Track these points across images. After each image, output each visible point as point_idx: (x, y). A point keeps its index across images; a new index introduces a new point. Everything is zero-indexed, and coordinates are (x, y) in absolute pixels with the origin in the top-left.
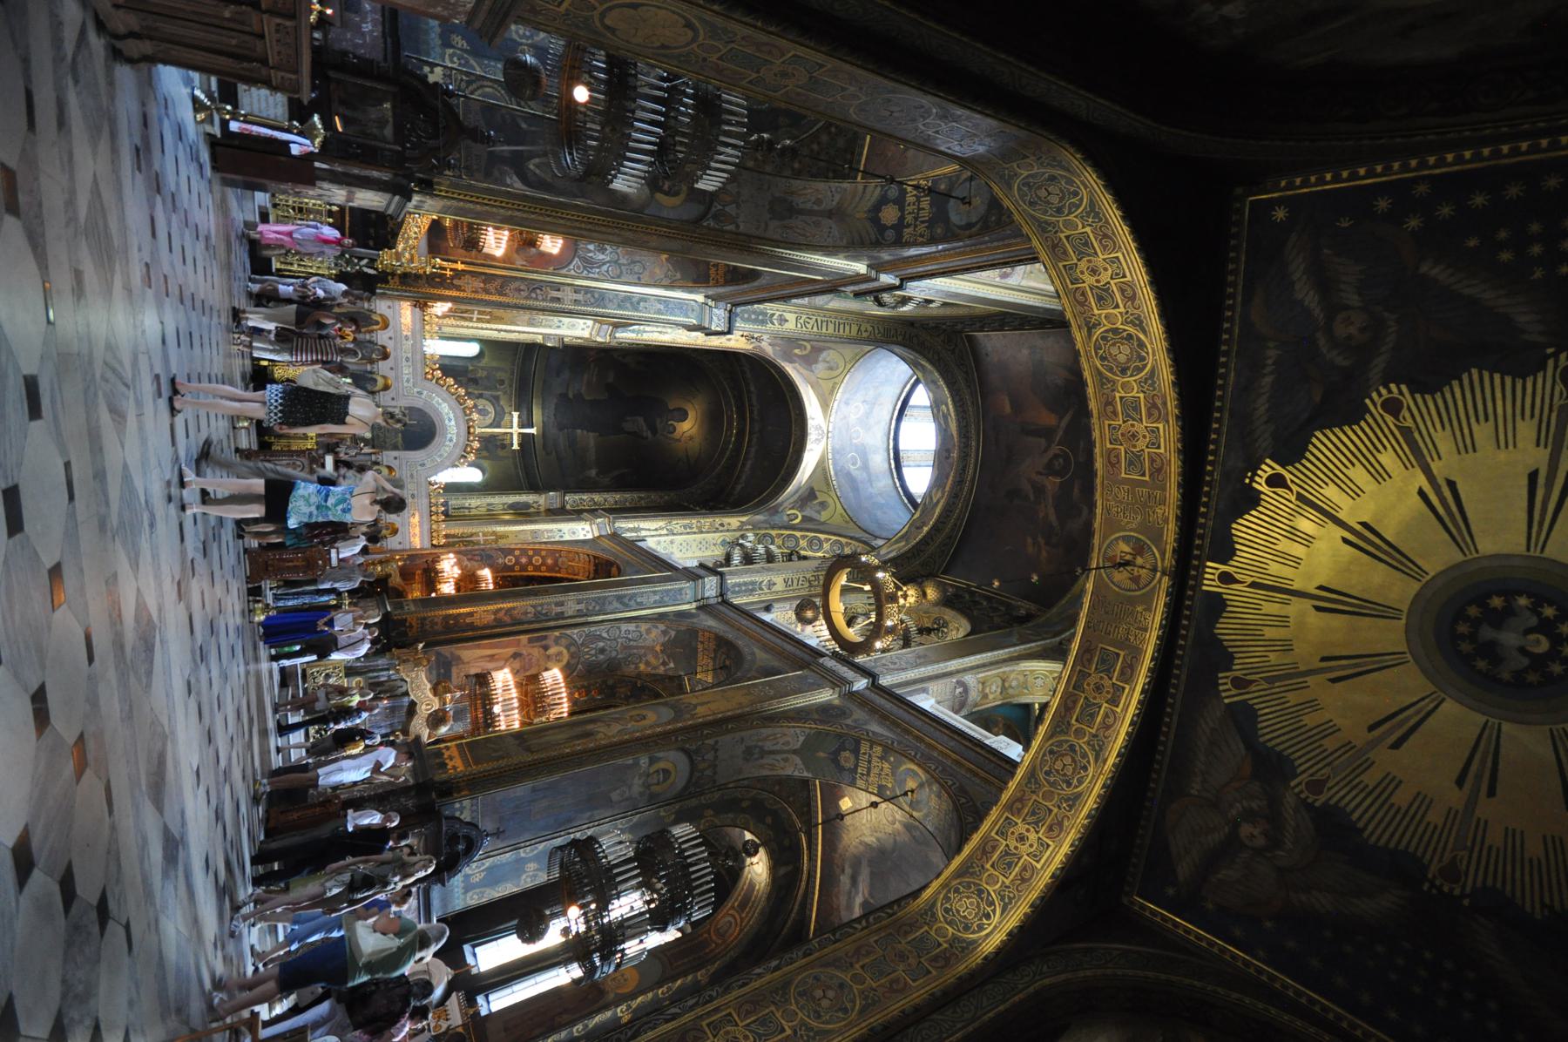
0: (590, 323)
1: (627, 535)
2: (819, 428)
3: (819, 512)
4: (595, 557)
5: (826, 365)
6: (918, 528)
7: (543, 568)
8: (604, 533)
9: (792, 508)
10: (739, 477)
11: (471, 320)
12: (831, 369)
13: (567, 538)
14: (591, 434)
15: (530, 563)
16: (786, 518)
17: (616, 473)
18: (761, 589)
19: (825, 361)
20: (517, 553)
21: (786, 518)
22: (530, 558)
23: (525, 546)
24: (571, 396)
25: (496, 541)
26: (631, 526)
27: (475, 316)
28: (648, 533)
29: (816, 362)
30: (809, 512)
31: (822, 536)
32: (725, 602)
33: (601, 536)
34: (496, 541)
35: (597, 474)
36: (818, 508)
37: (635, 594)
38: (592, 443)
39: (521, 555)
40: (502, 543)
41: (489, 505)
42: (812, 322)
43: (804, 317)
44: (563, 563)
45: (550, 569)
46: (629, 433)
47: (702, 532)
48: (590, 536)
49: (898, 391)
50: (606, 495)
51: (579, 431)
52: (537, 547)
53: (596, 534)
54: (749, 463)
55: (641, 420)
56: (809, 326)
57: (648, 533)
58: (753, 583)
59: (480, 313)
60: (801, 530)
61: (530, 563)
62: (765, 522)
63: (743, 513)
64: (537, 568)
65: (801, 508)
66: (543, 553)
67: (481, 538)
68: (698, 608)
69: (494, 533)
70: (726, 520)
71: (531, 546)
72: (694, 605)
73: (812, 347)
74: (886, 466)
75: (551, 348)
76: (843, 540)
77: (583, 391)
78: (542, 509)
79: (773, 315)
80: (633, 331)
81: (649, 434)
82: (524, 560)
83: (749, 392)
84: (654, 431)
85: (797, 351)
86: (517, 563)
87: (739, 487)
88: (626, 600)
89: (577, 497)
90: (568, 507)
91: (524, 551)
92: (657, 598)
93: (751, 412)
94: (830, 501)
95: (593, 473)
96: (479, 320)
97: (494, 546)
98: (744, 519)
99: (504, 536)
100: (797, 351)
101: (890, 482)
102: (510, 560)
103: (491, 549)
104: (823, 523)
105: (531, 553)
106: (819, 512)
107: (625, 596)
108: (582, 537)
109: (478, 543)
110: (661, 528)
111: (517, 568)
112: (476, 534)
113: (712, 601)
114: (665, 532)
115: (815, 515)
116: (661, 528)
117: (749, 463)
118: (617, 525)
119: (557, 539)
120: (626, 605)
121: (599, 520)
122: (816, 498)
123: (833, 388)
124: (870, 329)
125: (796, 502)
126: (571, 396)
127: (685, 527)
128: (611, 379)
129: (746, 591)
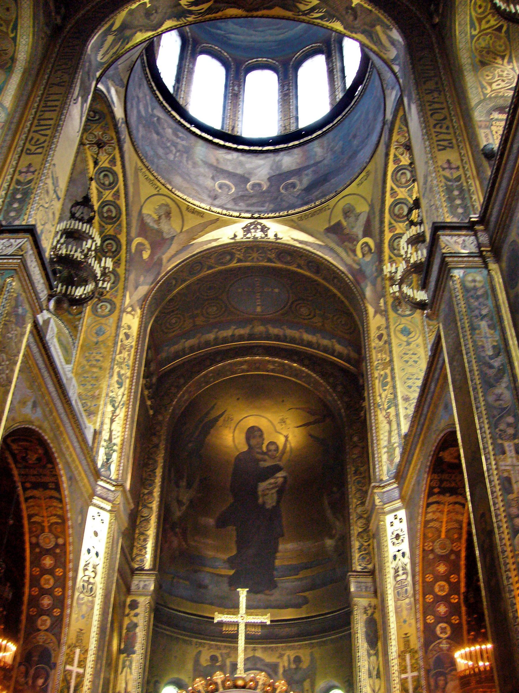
0: (92, 511)
1: (397, 459)
2: (247, 229)
3: (358, 215)
4: (430, 494)
5: (163, 220)
6: (355, 18)
7: (453, 578)
8: (396, 493)
9: (354, 251)
10: (326, 350)
11: (80, 677)
12: (168, 214)
13: (405, 547)
14: (281, 547)
15: (445, 599)
16: (368, 258)
17: (329, 513)
18: (459, 179)
19: (158, 221)
20: (430, 619)
21: (368, 258)
22: (438, 599)
23: (420, 606)
24: (231, 572)
25: (413, 652)
26: (385, 457)
27: (75, 669)
28: (395, 433)
29: (159, 232)
30: (359, 230)
31: (389, 201)
32: (483, 220)
33: (402, 497)
34: (413, 652)
35: (331, 537)
36: (352, 219)
37: (479, 359)
38: (290, 546)
39: (434, 613)
40: (416, 643)
41: (370, 676)
42: (37, 136)
43: (28, 145)
44: (443, 547)
45: (454, 568)
46: (278, 502)
47: (391, 361)
48: (402, 514)
49: (201, 142)
50: (353, 517)
51: (277, 563)
52: (419, 587)
53: (398, 504)
54: (306, 337)
55: (262, 486)
56: (42, 139)
57: (395, 433)
58: (449, 190)
59: (70, 662)
60: (382, 232)
61: (445, 599)
62: (374, 285)
63: (363, 313)
64: (454, 588)
65: (354, 240)
66: (429, 578)
67: (410, 675)
68: (498, 258)
69: (401, 656)
70: (373, 333)
71: (419, 597)
72: (493, 266)
73: (139, 235)
74: (296, 151)
75: (159, 587)
76: (391, 167)
77: (226, 557)
78: (374, 602)
79: (18, 182)
80: (109, 457)
81: (280, 474)
82: (442, 609)
83: (216, 341)
84: (277, 469)
85: (146, 255)
86: (445, 619)
87: (338, 347)
88: (491, 372)
89: (356, 555)
90: (370, 566)
91: (428, 608)
92: (483, 324)
93: (241, 338)
94: (342, 204)
95: (329, 543)
96: (82, 664)
97: (420, 654)
98: (371, 310)
99: (405, 640)
100: (146, 255)
101: (316, 142)
102: (443, 630)
103: (426, 658)
104: (372, 206)
105: (430, 598)
106: (358, 215)
107: (483, 375)
108: (404, 526)
109: (417, 680)
110: (387, 416)
111: (455, 620)
112: (403, 683)
113: (484, 238)
114: (392, 411)
115: (363, 219)
116: (387, 416)
117: (306, 337)
118: (385, 478)
119: (407, 560)
120: (501, 372)
121: (377, 501)
122: (339, 224)
123: (193, 211)
124: (59, 74)
125: (345, 249)
126: (231, 572)
127: (385, 385)
128: (211, 521)
129: (463, 199)
